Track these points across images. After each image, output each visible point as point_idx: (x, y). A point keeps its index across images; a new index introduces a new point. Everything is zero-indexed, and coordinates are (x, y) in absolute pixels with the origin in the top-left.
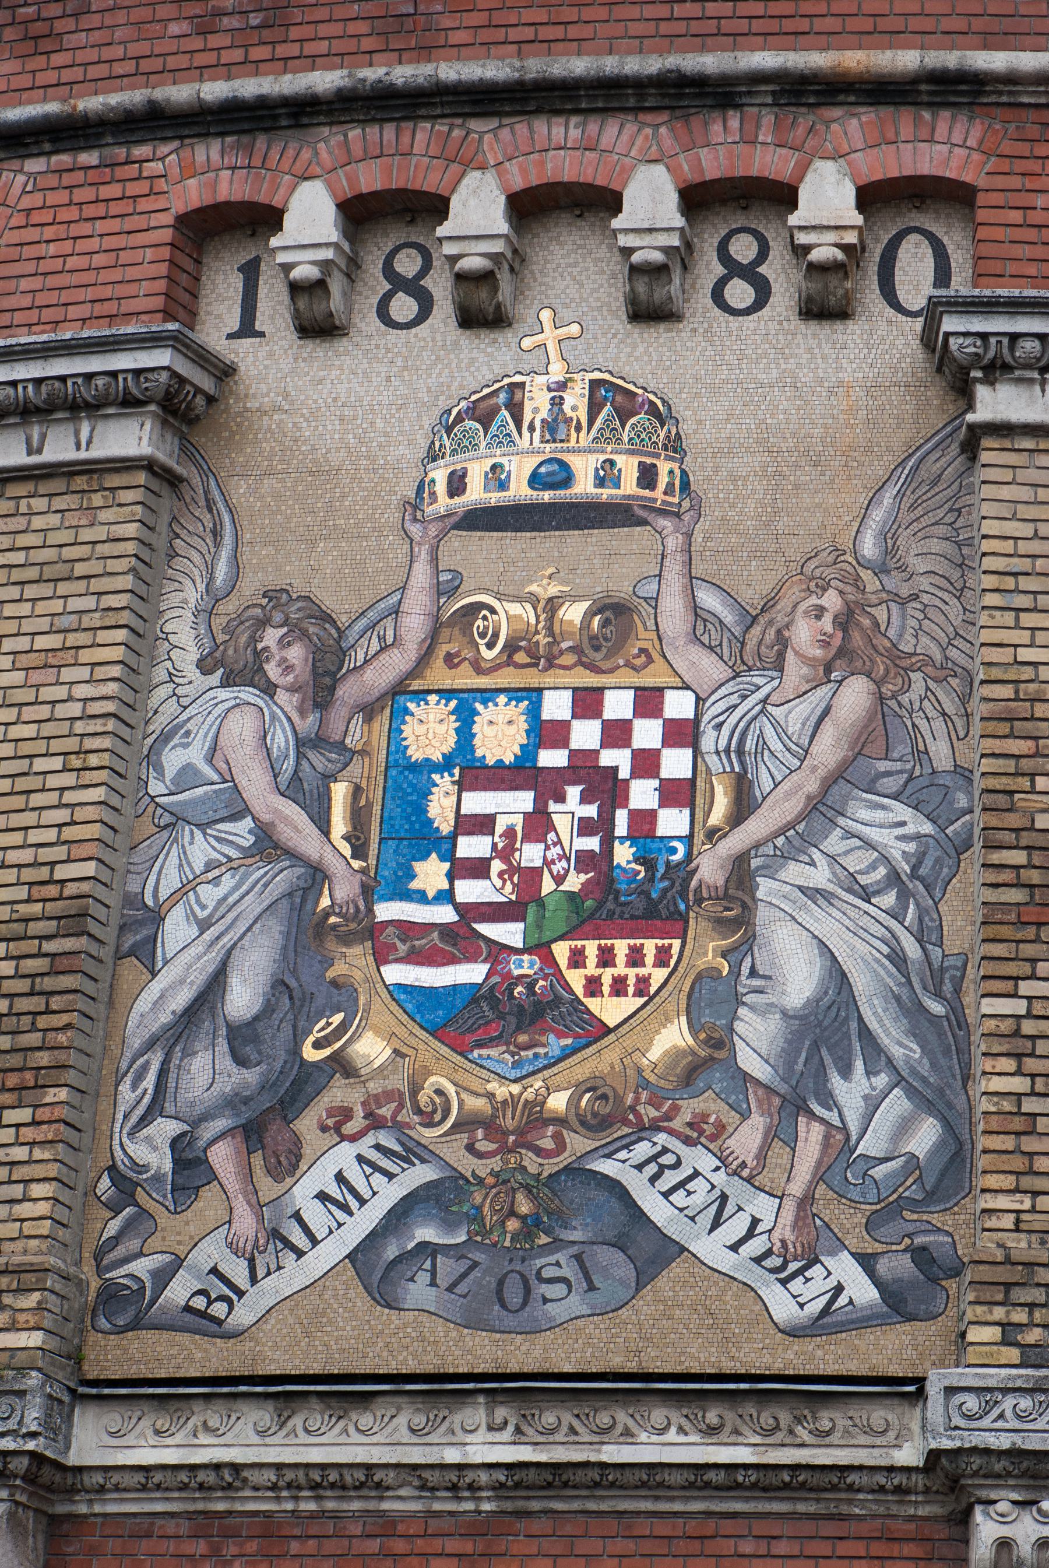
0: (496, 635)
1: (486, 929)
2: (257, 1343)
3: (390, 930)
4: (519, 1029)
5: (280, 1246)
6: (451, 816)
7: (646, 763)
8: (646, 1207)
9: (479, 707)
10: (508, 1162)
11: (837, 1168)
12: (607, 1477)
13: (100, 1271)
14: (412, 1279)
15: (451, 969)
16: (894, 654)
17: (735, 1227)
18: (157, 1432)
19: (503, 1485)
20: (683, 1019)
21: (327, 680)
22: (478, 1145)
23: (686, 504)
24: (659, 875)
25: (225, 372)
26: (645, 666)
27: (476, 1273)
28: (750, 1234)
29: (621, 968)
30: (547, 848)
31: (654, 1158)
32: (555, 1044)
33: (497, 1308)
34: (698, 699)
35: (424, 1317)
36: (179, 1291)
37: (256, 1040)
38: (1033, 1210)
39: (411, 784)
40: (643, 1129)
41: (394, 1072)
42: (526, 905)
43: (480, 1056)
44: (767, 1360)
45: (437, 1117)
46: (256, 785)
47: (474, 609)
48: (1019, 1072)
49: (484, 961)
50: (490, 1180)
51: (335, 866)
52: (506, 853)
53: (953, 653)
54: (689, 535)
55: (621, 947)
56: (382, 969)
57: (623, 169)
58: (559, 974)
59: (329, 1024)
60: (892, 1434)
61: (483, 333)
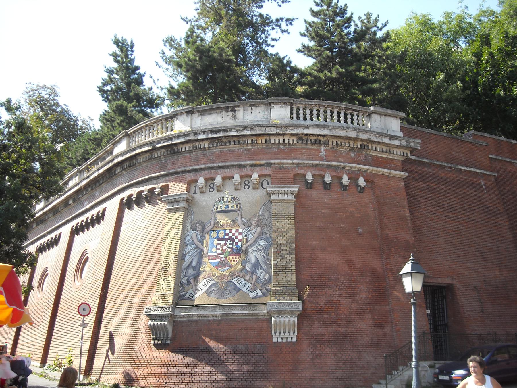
7: (237, 237)
12: (233, 315)
16: (263, 225)
17: (246, 287)
25: (193, 197)
32: (227, 268)
36: (187, 296)
46: (196, 241)
47: (218, 222)
55: (234, 257)
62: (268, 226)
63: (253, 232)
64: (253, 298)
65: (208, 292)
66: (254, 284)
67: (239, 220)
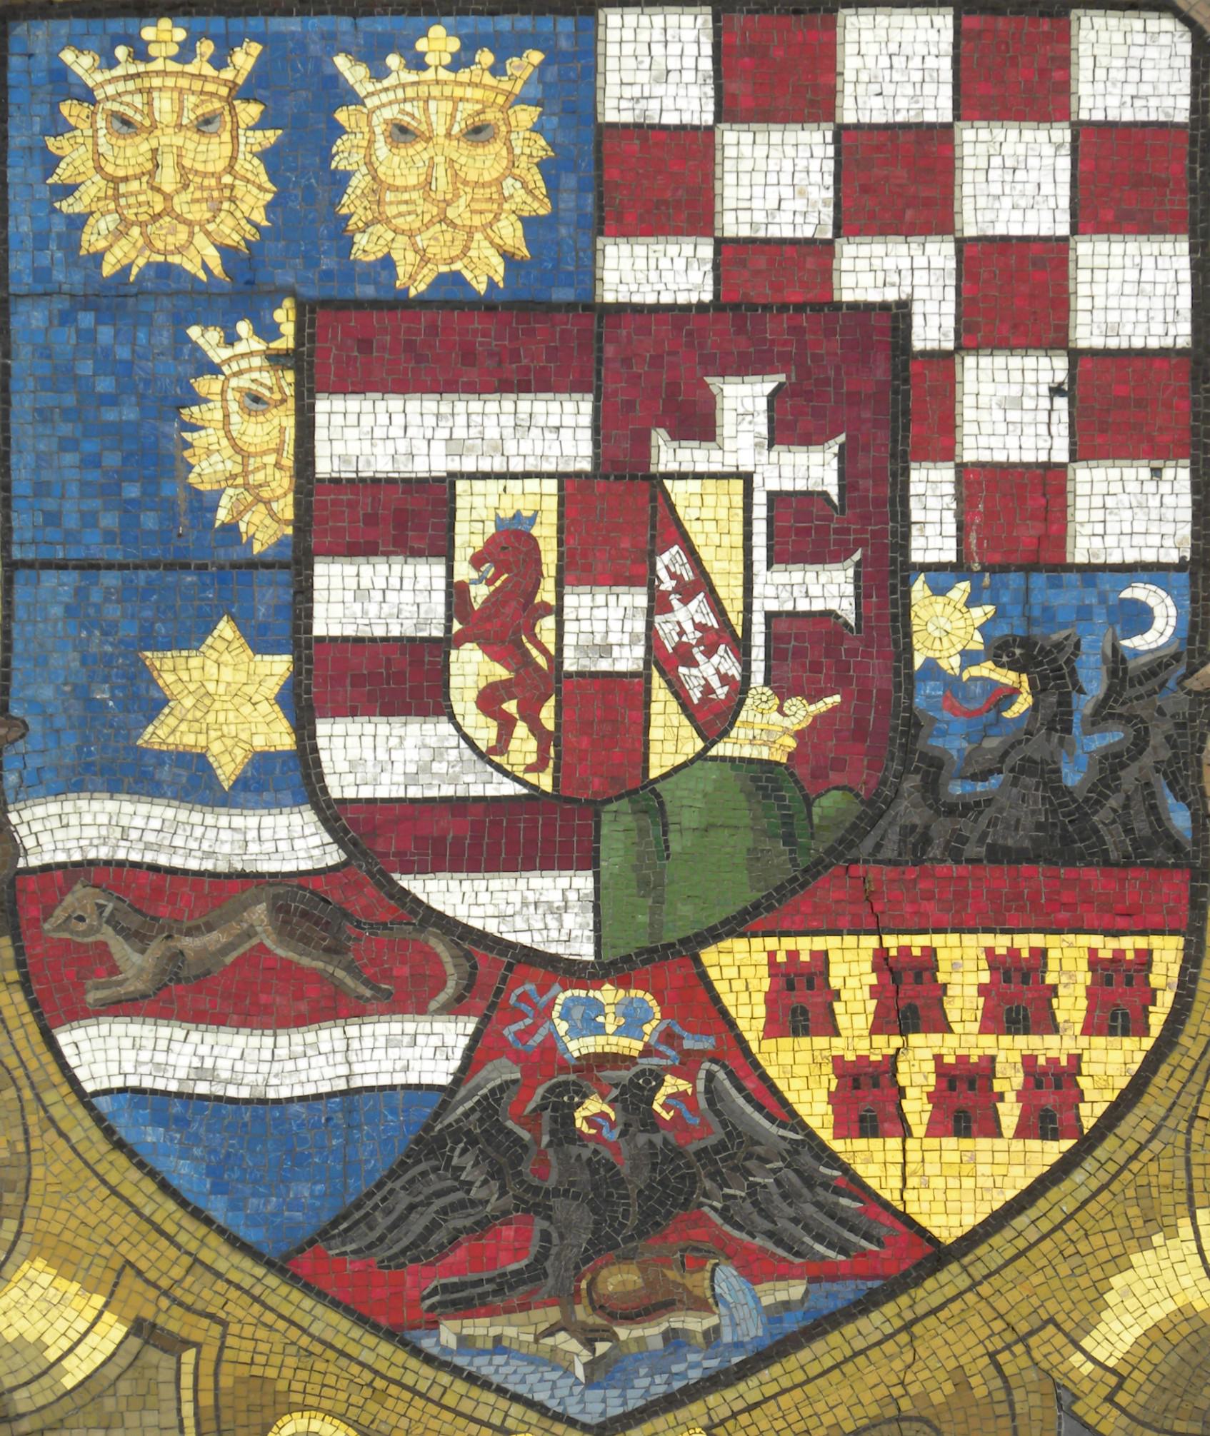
1: (443, 892)
3: (80, 897)
4: (602, 1247)
6: (281, 484)
7: (1016, 293)
9: (349, 69)
15: (328, 1036)
24: (1084, 705)
29: (966, 1038)
30: (658, 604)
32: (741, 1304)
39: (105, 361)
41: (144, 1400)
42: (593, 809)
43: (464, 1341)
49: (456, 1008)
52: (504, 620)
55: (963, 962)
56: (64, 1038)
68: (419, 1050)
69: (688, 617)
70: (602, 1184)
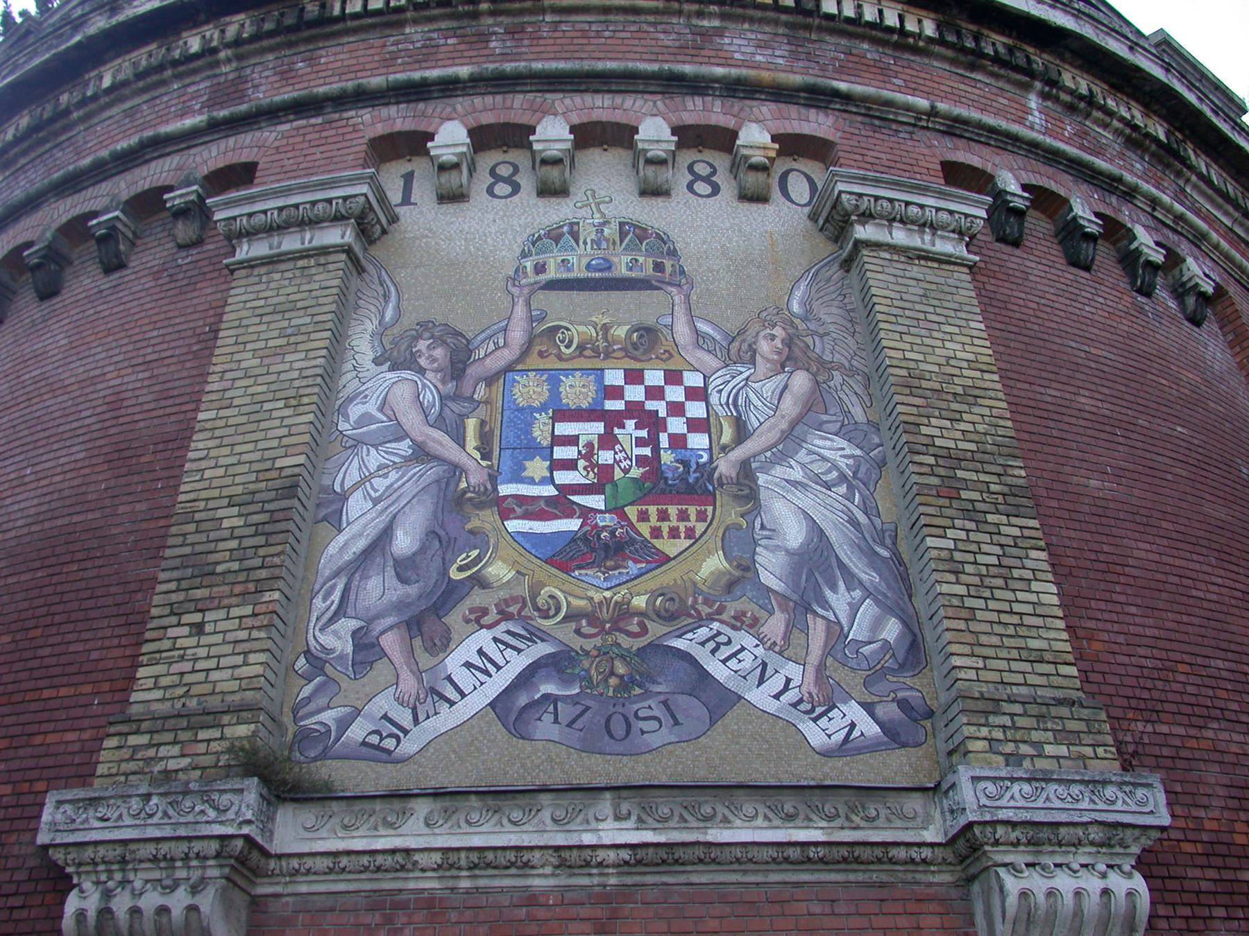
0: (571, 342)
2: (420, 766)
4: (607, 557)
5: (436, 698)
8: (710, 669)
10: (606, 640)
11: (839, 647)
12: (711, 854)
13: (296, 720)
14: (539, 719)
16: (820, 361)
17: (776, 683)
18: (345, 827)
19: (626, 863)
20: (721, 552)
21: (461, 366)
22: (583, 630)
23: (684, 281)
25: (394, 219)
26: (668, 359)
27: (588, 714)
28: (786, 688)
29: (674, 523)
31: (712, 638)
32: (633, 568)
33: (607, 738)
34: (705, 377)
35: (551, 745)
36: (357, 732)
37: (415, 567)
38: (985, 668)
40: (702, 619)
42: (604, 485)
44: (811, 773)
45: (552, 612)
46: (412, 420)
47: (556, 329)
48: (958, 582)
50: (594, 653)
51: (471, 465)
52: (589, 455)
53: (854, 363)
54: (688, 297)
55: (673, 510)
57: (637, 117)
58: (631, 525)
59: (468, 556)
60: (919, 820)
61: (552, 200)
62: (851, 372)
63: (769, 387)
64: (826, 754)
65: (511, 711)
66: (821, 668)
67: (682, 331)
68: (573, 524)
69: (620, 456)
70: (606, 547)
